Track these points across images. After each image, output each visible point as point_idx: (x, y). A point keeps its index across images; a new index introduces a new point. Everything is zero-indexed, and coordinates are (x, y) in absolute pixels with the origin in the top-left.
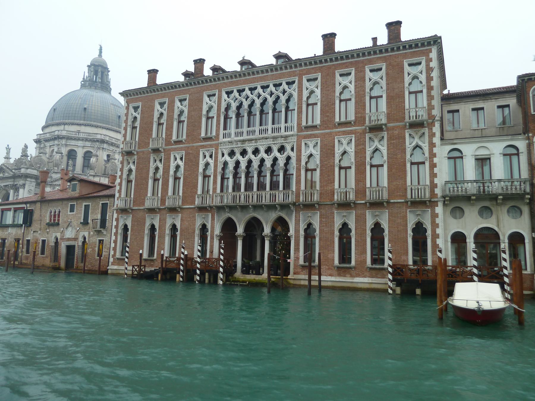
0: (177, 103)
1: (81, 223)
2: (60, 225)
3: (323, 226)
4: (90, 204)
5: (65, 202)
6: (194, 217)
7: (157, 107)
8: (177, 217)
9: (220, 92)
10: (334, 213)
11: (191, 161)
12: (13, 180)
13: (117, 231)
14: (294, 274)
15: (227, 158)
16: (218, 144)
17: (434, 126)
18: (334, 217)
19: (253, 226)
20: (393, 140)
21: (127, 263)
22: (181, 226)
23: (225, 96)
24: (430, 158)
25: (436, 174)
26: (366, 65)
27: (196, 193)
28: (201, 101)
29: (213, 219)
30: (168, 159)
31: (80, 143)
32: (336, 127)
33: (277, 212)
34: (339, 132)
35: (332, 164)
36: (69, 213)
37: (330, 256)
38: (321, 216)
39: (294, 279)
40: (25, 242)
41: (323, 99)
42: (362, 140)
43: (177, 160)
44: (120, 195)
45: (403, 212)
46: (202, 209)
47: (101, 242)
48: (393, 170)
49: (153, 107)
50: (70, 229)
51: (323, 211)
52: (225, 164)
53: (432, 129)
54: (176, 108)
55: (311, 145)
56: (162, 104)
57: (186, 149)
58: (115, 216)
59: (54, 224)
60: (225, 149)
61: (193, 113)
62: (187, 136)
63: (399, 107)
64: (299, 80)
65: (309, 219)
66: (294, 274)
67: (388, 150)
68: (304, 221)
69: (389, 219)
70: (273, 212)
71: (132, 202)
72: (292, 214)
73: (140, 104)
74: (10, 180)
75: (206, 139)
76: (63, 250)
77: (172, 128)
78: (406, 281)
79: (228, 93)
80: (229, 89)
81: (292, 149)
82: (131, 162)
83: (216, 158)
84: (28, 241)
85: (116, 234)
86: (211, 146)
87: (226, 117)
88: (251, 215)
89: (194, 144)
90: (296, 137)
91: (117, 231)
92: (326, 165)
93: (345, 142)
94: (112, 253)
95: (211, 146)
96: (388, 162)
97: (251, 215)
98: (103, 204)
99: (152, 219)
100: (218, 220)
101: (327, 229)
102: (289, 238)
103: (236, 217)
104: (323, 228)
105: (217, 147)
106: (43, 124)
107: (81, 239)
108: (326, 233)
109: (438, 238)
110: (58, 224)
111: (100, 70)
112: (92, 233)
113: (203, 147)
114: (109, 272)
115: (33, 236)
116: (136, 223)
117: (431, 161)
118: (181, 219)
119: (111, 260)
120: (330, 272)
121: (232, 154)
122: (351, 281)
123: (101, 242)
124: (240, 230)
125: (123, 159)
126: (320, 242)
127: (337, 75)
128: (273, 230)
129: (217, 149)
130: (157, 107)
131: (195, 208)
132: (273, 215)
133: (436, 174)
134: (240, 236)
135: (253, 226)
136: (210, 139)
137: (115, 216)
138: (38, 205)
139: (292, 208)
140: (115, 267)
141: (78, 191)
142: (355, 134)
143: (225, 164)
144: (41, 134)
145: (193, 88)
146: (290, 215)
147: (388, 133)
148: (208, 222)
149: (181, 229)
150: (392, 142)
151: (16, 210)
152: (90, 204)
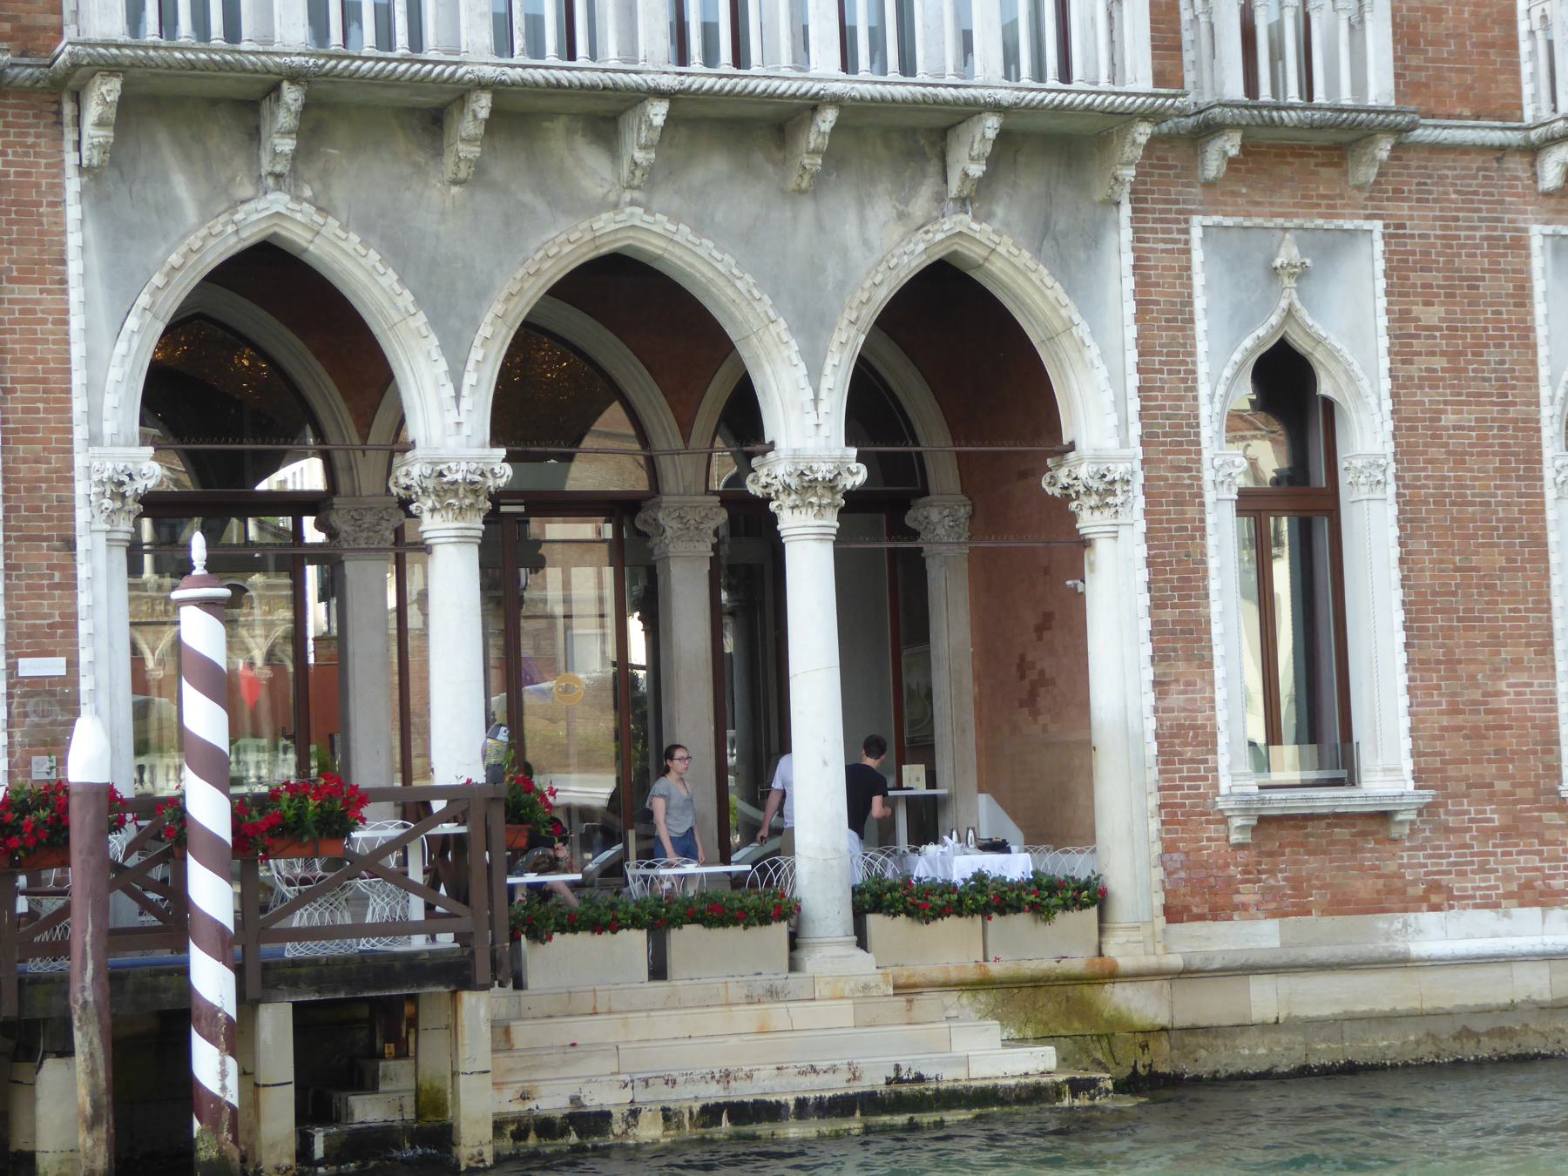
10: (1520, 244)
14: (1173, 914)
33: (920, 205)
37: (1509, 691)
38: (1397, 270)
39: (1186, 973)
51: (1421, 222)
65: (1289, 295)
66: (1173, 914)
70: (882, 209)
72: (1093, 239)
88: (605, 223)
97: (605, 223)
100: (122, 286)
101: (1469, 416)
103: (399, 254)
104: (1425, 397)
108: (1459, 458)
120: (1523, 862)
128: (871, 411)
132: (880, 243)
134: (444, 490)
146: (1069, 251)
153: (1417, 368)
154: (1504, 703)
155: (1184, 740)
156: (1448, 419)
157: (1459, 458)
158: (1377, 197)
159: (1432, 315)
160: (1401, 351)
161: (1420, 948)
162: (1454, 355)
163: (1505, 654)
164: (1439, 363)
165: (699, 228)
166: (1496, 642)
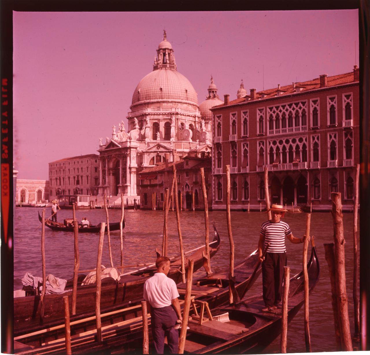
0: (242, 114)
7: (231, 116)
23: (268, 110)
26: (342, 93)
31: (161, 117)
49: (229, 116)
54: (242, 117)
56: (234, 115)
64: (308, 102)
79: (271, 109)
81: (306, 140)
85: (215, 188)
94: (214, 198)
106: (130, 104)
111: (167, 53)
114: (213, 208)
119: (214, 202)
127: (328, 99)
130: (231, 116)
136: (263, 135)
137: (213, 178)
140: (216, 206)
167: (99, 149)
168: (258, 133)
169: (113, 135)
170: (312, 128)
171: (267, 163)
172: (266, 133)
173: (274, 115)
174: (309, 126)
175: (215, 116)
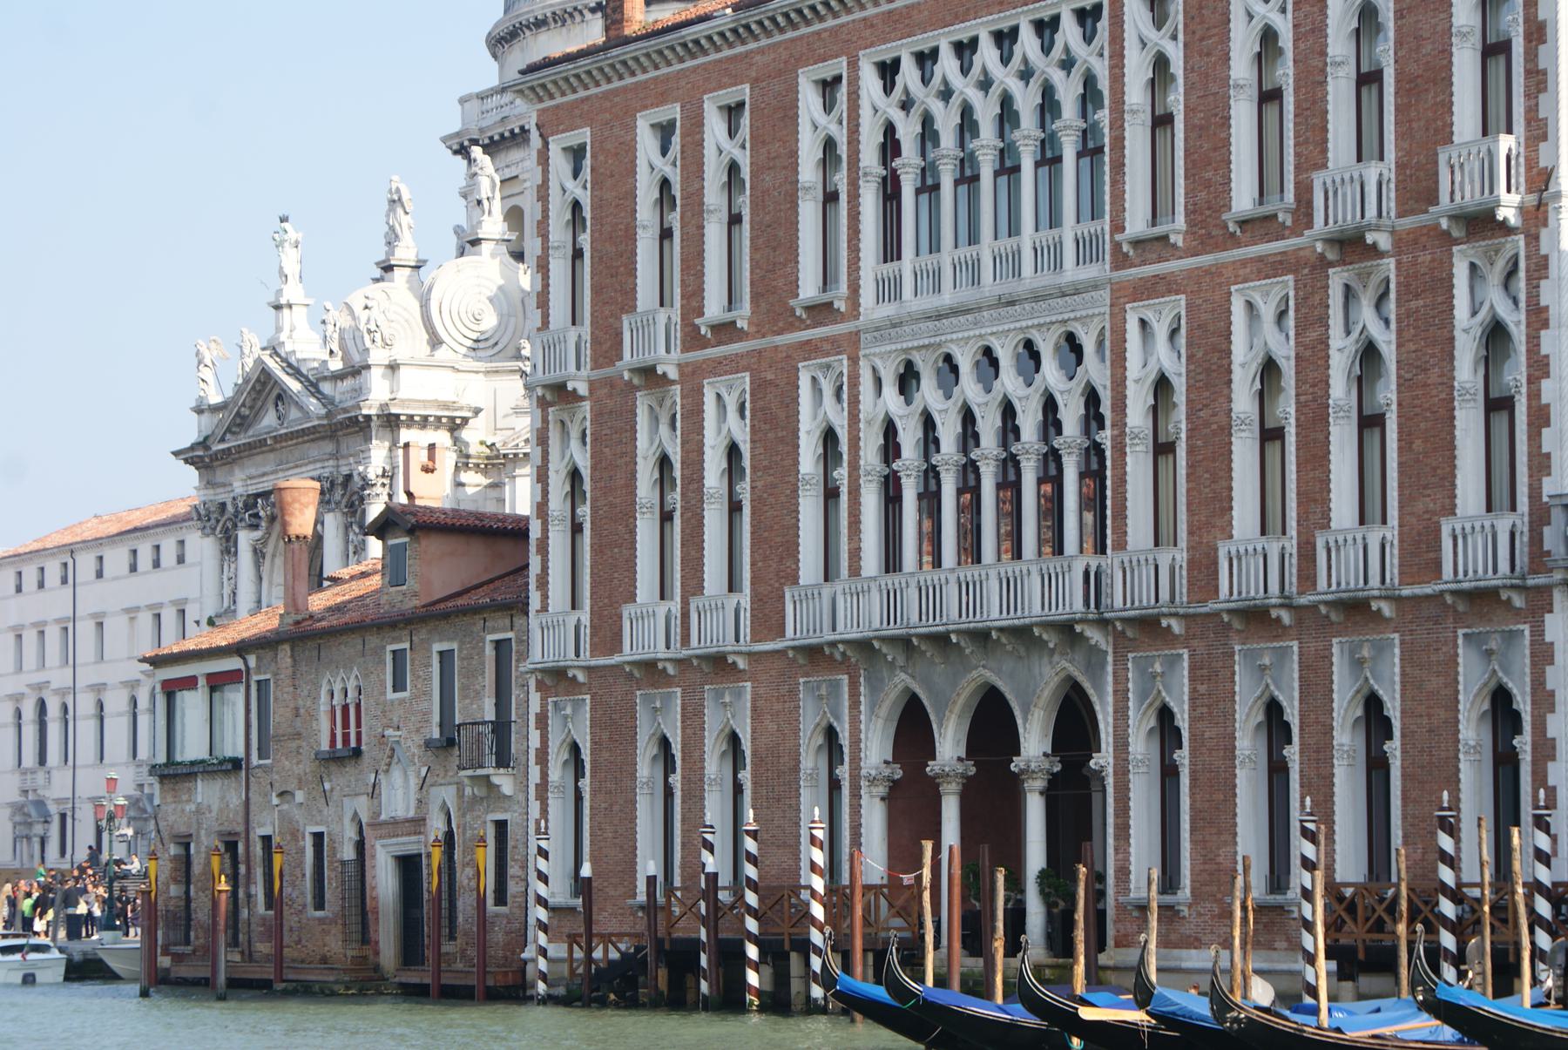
0: (715, 126)
1: (428, 744)
2: (366, 758)
3: (1201, 718)
4: (455, 646)
5: (373, 641)
6: (793, 693)
8: (739, 694)
9: (854, 65)
10: (1233, 654)
11: (773, 414)
12: (329, 447)
13: (544, 775)
15: (891, 399)
16: (857, 333)
17: (1546, 225)
18: (1234, 673)
19: (993, 725)
20: (1417, 296)
21: (544, 927)
22: (753, 739)
23: (870, 82)
24: (1529, 382)
25: (1548, 456)
27: (794, 580)
28: (788, 113)
29: (855, 705)
30: (694, 414)
32: (1232, 241)
34: (1244, 263)
35: (1224, 420)
36: (391, 695)
40: (258, 849)
41: (1193, 98)
42: (1317, 297)
43: (725, 423)
44: (545, 597)
45: (1446, 643)
46: (814, 655)
47: (501, 826)
48: (1418, 444)
49: (631, 148)
50: (396, 774)
52: (890, 430)
53: (1537, 238)
55: (1161, 331)
57: (751, 363)
58: (535, 700)
59: (347, 755)
60: (881, 356)
61: (768, 177)
62: (755, 297)
63: (1436, 130)
67: (1399, 346)
68: (1143, 696)
69: (1403, 674)
71: (586, 634)
73: (584, 135)
74: (315, 450)
75: (821, 311)
76: (385, 881)
77: (700, 254)
78: (1361, 956)
79: (888, 71)
80: (885, 52)
82: (575, 434)
83: (854, 402)
84: (267, 840)
85: (543, 788)
86: (835, 345)
87: (890, 192)
89: (780, 340)
90: (1105, 295)
91: (544, 775)
92: (1207, 424)
93: (1268, 311)
95: (835, 345)
96: (1399, 405)
98: (498, 644)
99: (655, 709)
100: (873, 707)
102: (1099, 776)
105: (851, 345)
107: (436, 826)
108: (1210, 750)
109: (1553, 758)
110: (357, 753)
112: (468, 791)
113: (810, 349)
115: (283, 817)
116: (605, 736)
117: (1534, 395)
118: (754, 709)
121: (908, 380)
122: (1284, 967)
123: (501, 826)
124: (949, 746)
125: (545, 420)
126: (1192, 795)
129: (854, 361)
131: (781, 653)
133: (1548, 456)
135: (993, 725)
138: (285, 652)
139: (1095, 636)
141: (412, 584)
142: (1295, 272)
143: (890, 430)
144: (482, 97)
145: (761, 51)
147: (1399, 263)
148: (837, 718)
149: (754, 754)
150: (1413, 304)
151: (217, 683)
152: (455, 646)
153: (1200, 710)
154: (1220, 859)
155: (1123, 872)
156: (1207, 735)
157: (1210, 750)
158: (1185, 641)
159: (1202, 688)
160: (1193, 708)
161: (1185, 965)
162: (1209, 706)
163: (1223, 838)
164: (1205, 710)
165: (998, 673)
166: (1219, 833)
167: (189, 431)
168: (809, 288)
169: (278, 307)
170: (1137, 243)
171: (855, 571)
172: (854, 288)
173: (908, 131)
174: (1118, 227)
175: (546, 144)
